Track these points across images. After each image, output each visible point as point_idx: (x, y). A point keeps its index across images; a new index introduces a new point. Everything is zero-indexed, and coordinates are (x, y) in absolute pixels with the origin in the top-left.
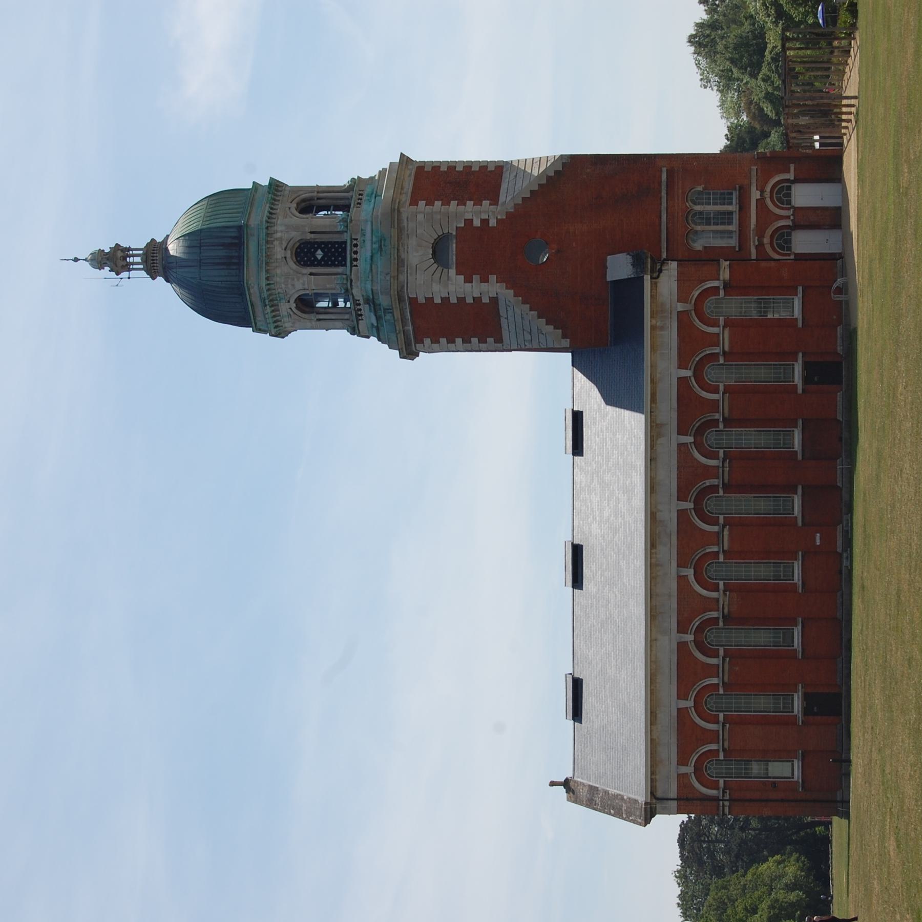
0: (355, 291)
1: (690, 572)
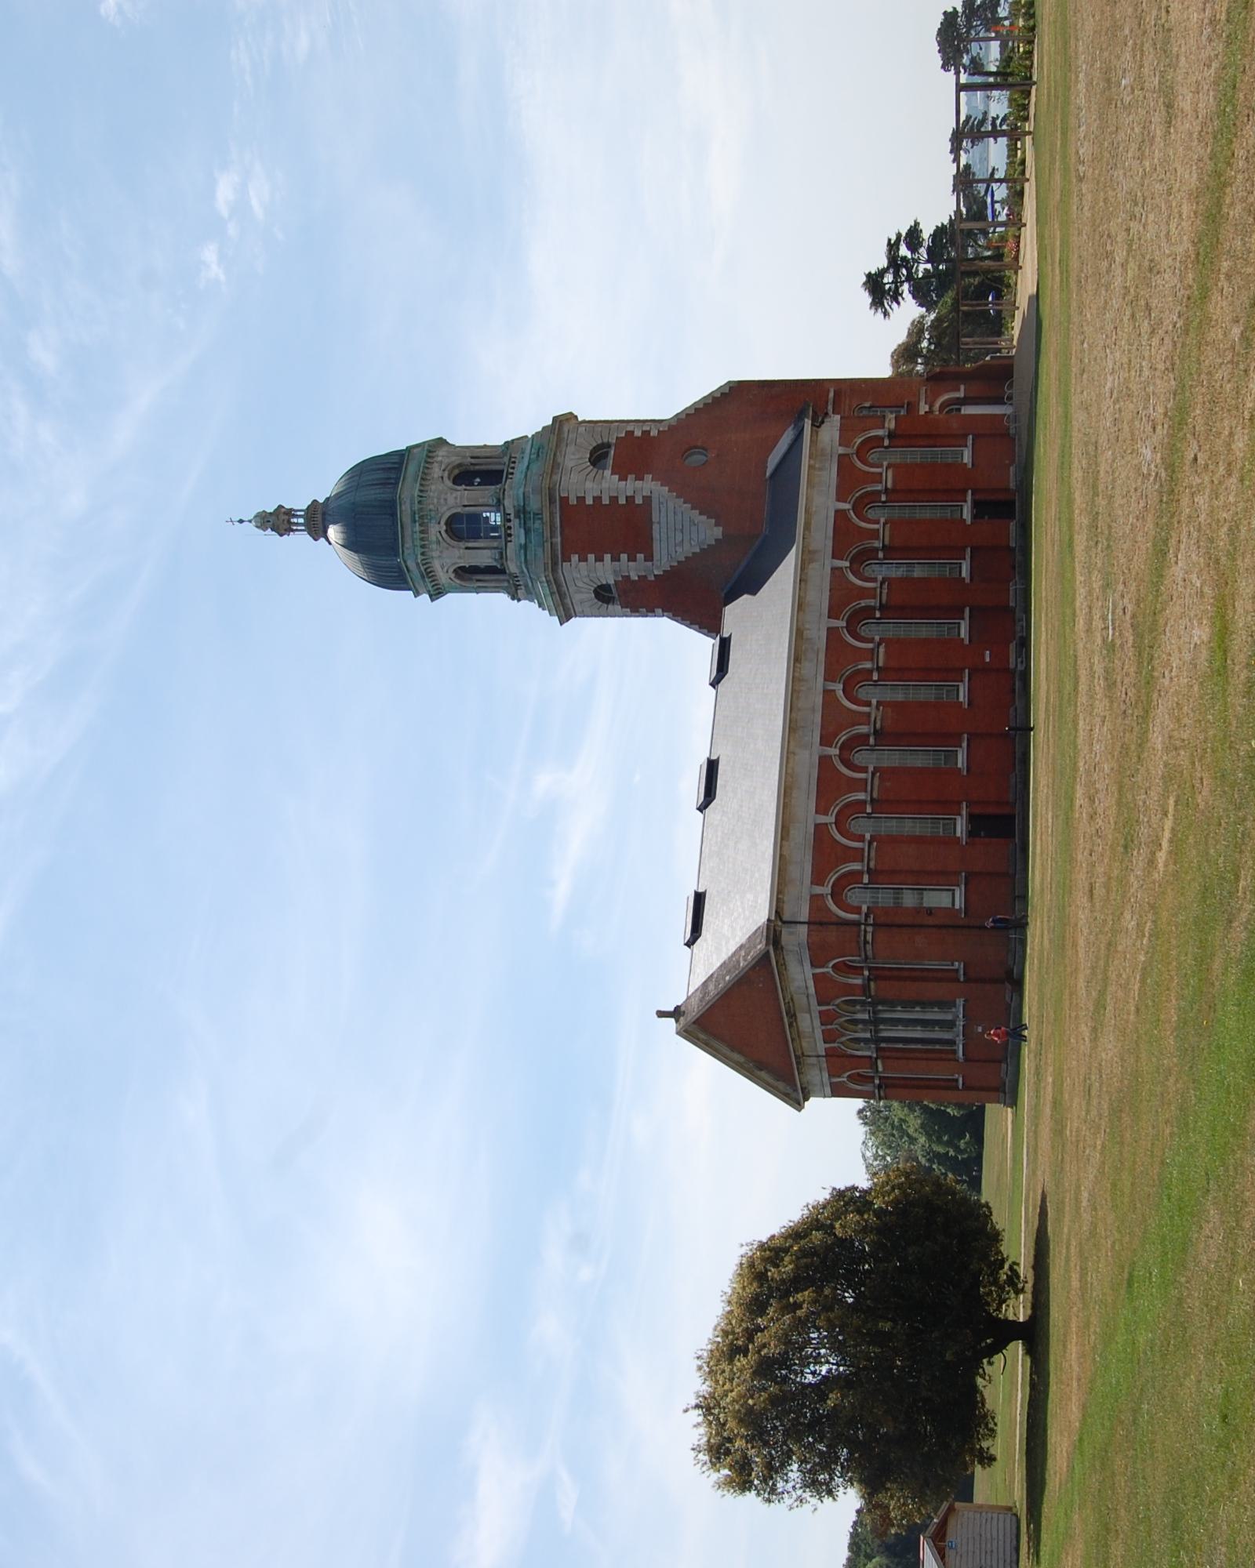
0: (506, 503)
1: (838, 688)
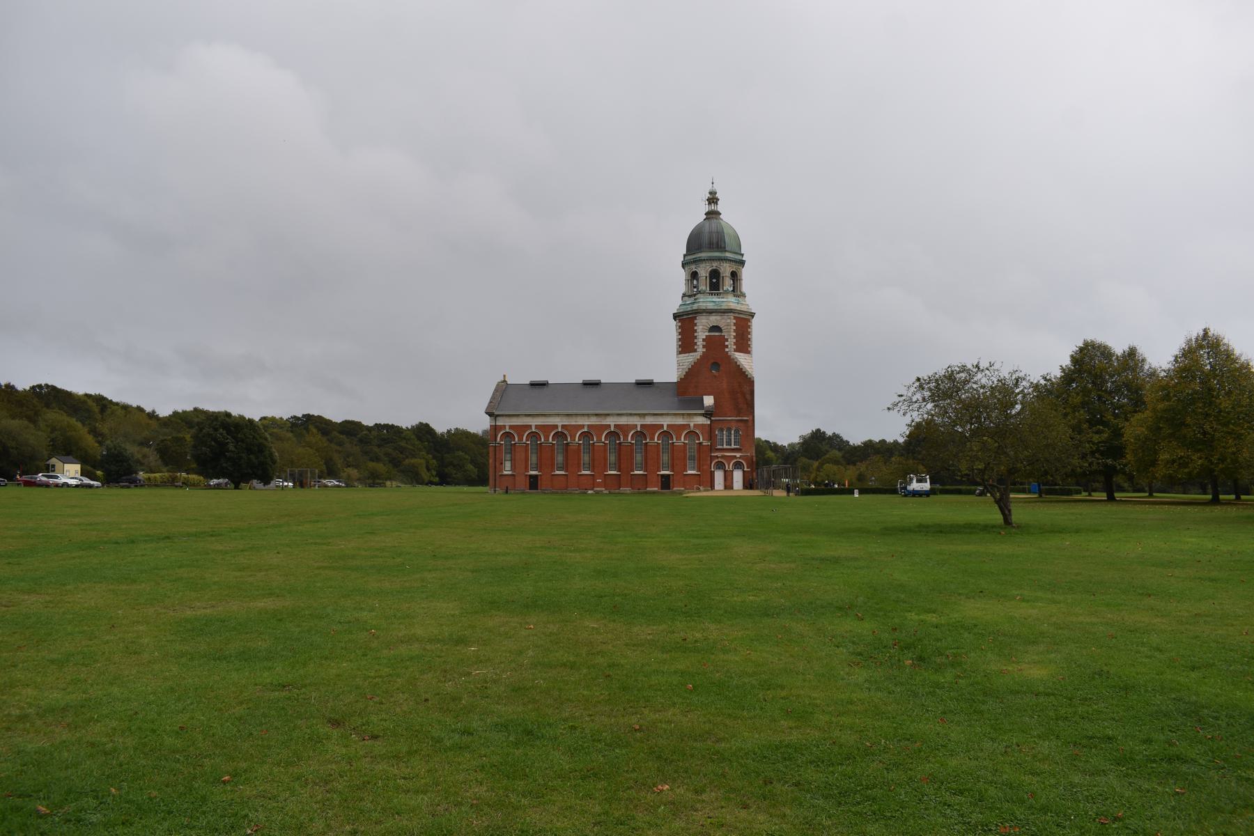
1: (586, 430)
